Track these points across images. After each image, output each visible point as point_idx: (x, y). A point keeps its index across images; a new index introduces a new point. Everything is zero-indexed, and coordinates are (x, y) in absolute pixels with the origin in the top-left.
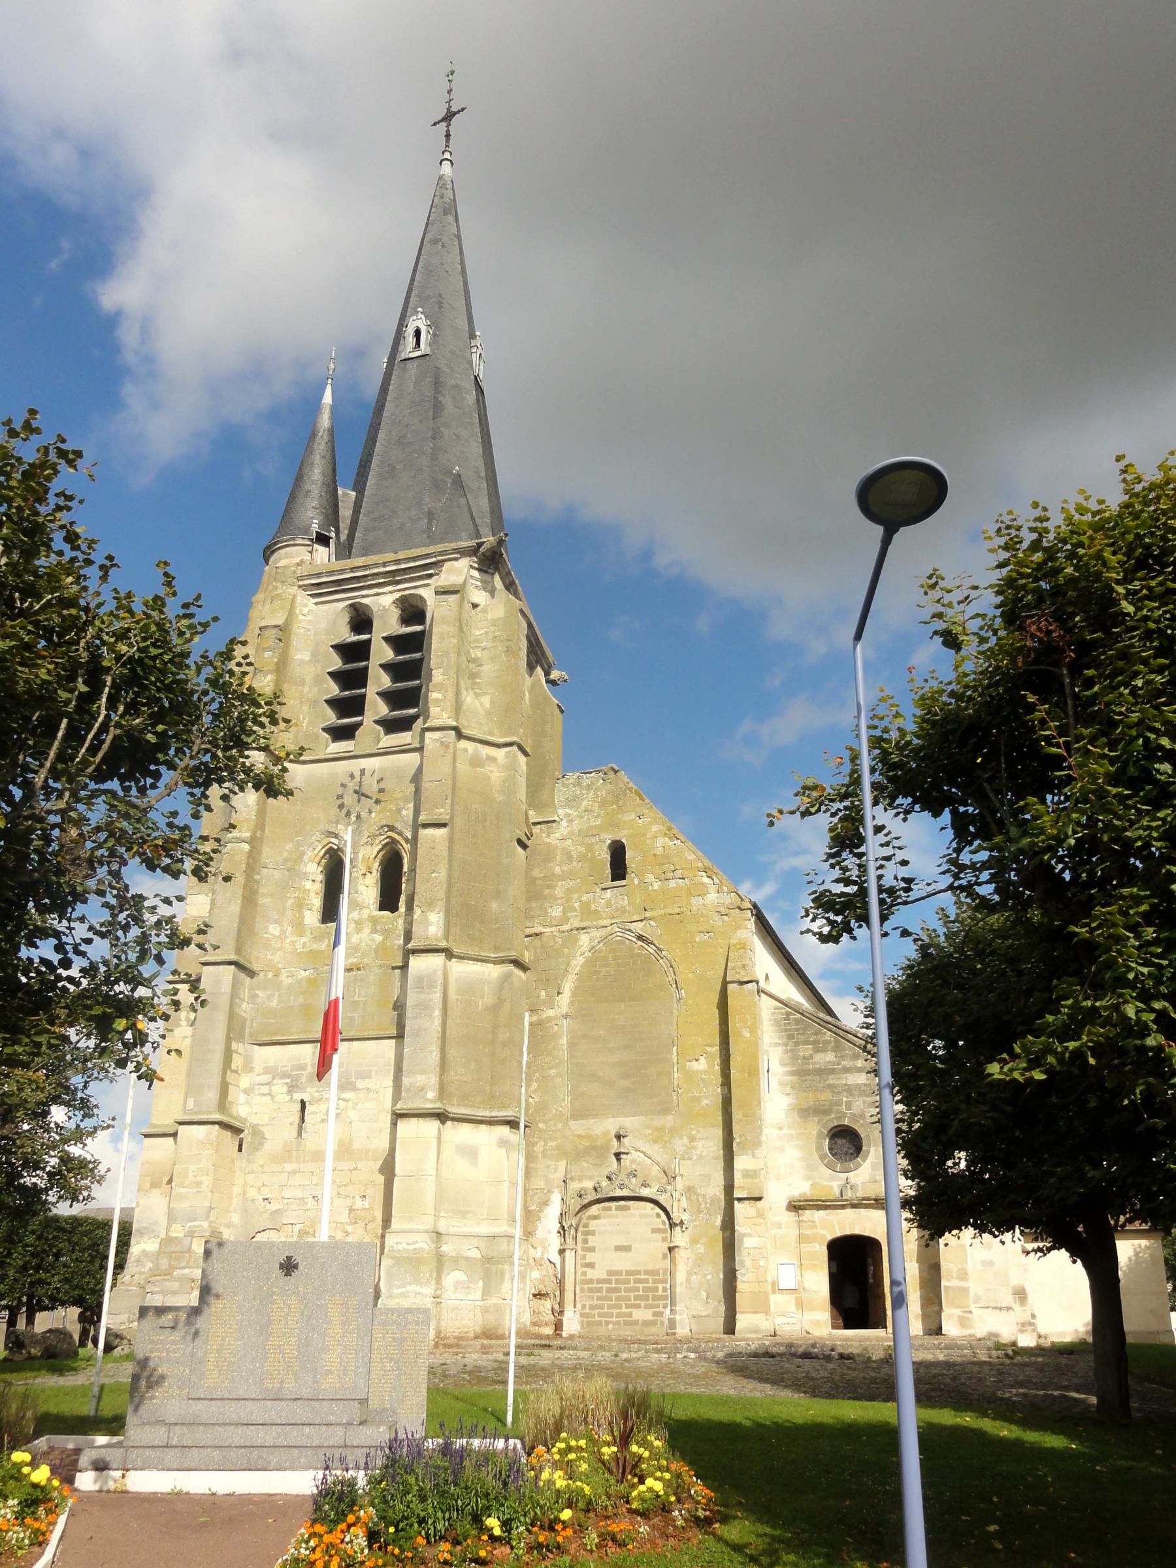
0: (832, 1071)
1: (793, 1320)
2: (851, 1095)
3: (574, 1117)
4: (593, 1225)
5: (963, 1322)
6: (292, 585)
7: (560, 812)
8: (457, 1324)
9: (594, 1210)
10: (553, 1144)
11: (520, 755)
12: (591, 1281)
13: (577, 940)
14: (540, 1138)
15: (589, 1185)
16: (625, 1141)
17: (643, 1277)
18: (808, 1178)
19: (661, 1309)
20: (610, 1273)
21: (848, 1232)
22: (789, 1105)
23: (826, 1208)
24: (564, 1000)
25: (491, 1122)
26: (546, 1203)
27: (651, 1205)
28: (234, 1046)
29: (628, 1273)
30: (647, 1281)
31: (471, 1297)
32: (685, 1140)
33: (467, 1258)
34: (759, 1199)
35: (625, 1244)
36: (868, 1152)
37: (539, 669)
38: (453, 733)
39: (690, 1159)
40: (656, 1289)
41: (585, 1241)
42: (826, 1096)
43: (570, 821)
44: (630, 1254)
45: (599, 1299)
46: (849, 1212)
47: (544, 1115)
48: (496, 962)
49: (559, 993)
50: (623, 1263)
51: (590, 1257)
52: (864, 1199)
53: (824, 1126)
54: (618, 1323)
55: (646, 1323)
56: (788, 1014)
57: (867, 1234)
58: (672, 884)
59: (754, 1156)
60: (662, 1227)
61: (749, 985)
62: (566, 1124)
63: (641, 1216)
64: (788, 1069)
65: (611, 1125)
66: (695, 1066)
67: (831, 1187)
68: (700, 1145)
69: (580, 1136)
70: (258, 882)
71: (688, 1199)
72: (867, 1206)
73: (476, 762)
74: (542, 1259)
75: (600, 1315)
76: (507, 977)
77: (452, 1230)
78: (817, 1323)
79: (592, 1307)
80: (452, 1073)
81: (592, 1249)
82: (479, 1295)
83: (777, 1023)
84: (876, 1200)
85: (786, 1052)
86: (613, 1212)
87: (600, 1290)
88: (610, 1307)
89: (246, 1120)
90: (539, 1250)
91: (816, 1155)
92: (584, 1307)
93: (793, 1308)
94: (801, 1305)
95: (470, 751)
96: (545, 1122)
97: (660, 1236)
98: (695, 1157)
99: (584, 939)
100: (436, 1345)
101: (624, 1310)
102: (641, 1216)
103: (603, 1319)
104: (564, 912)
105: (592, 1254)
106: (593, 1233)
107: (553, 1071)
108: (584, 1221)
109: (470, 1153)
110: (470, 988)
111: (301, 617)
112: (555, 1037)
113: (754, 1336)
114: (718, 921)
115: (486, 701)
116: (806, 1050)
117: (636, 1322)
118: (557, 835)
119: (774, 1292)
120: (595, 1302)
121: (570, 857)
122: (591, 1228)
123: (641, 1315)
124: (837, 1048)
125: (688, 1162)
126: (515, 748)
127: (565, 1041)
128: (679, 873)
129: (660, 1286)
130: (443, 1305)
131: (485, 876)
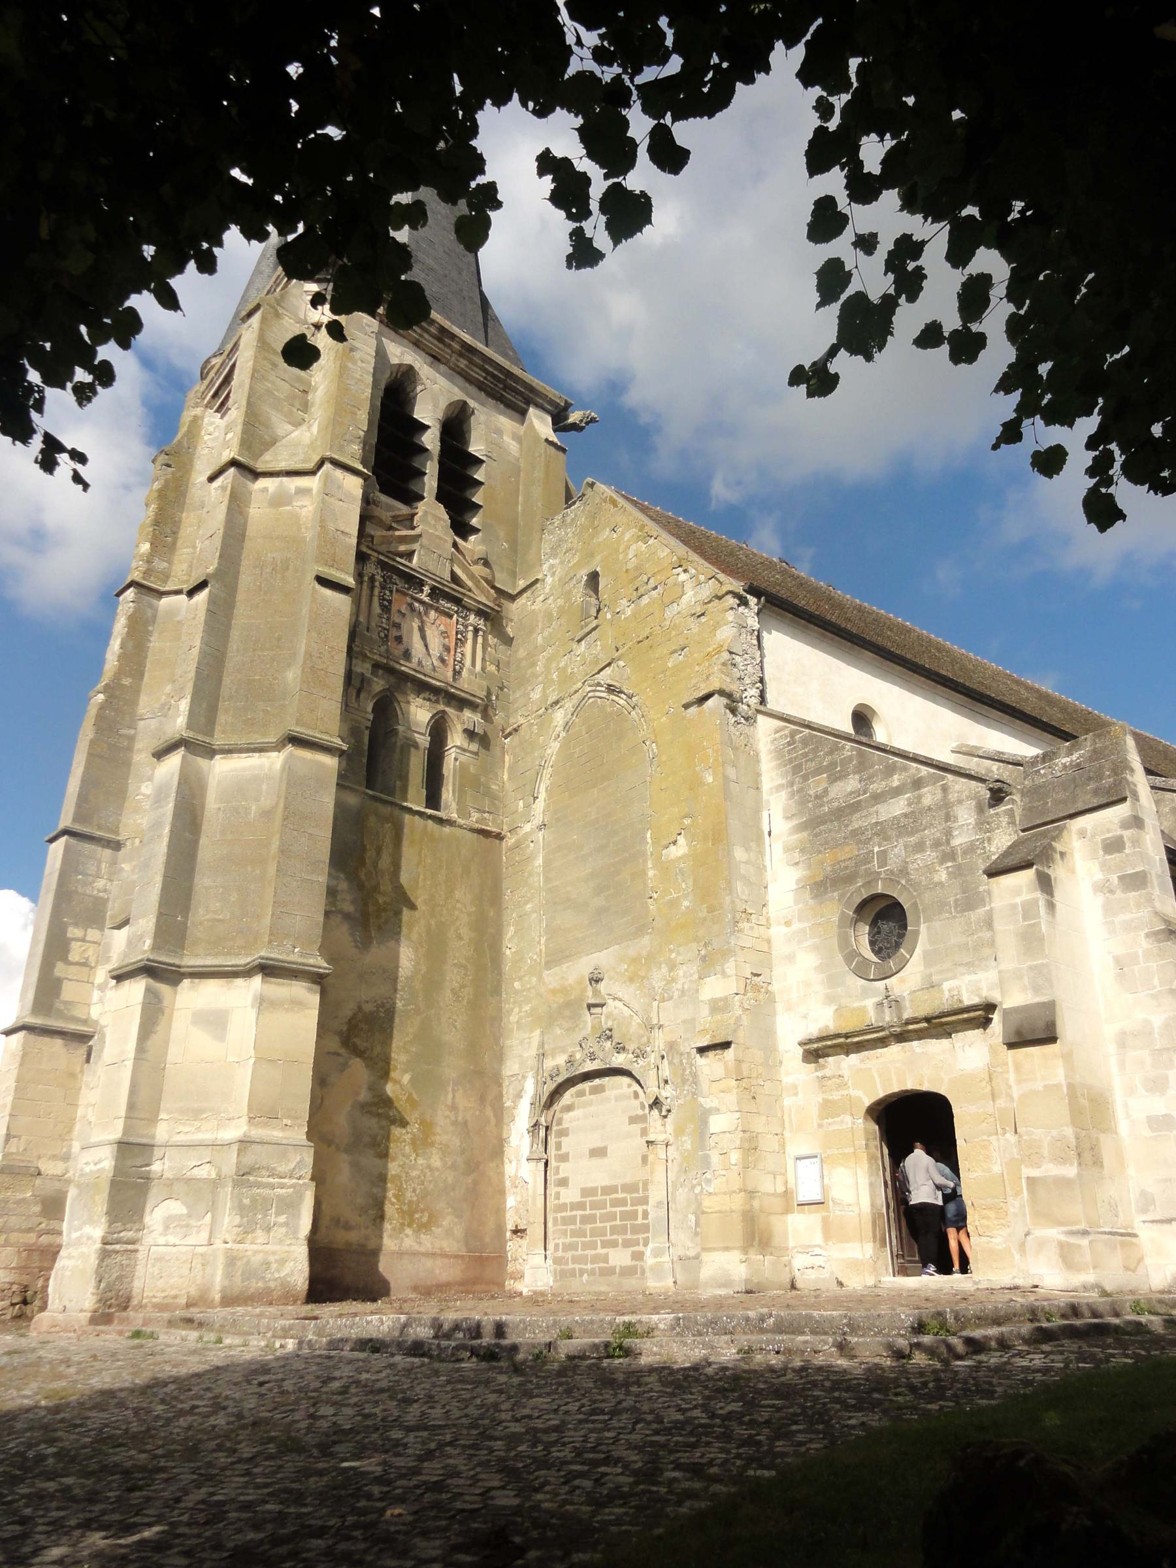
0: (855, 807)
1: (818, 1261)
2: (887, 838)
3: (549, 965)
4: (567, 1117)
5: (1067, 1257)
6: (197, 405)
7: (545, 567)
8: (160, 1283)
9: (568, 1097)
10: (527, 1008)
11: (339, 473)
12: (561, 1208)
13: (551, 720)
14: (515, 1002)
15: (561, 1060)
16: (602, 986)
17: (620, 1195)
18: (830, 999)
19: (641, 1248)
20: (586, 1192)
21: (895, 1088)
22: (798, 881)
23: (859, 1047)
24: (539, 806)
25: (246, 973)
26: (519, 1096)
27: (626, 1080)
28: (73, 932)
29: (607, 1190)
30: (623, 1202)
31: (191, 1240)
32: (664, 969)
33: (189, 1180)
34: (726, 1045)
36: (916, 933)
37: (532, 411)
38: (232, 470)
39: (670, 998)
40: (633, 1215)
41: (559, 1146)
42: (850, 851)
43: (553, 574)
44: (606, 1161)
45: (574, 1234)
46: (895, 1049)
48: (278, 747)
49: (535, 798)
50: (597, 1175)
51: (565, 1169)
52: (909, 1022)
53: (847, 904)
54: (592, 1273)
55: (628, 1272)
56: (793, 734)
57: (926, 1087)
58: (645, 600)
59: (724, 974)
60: (640, 1112)
61: (710, 702)
62: (540, 978)
63: (617, 1099)
64: (795, 822)
65: (583, 966)
66: (675, 852)
67: (863, 1009)
68: (681, 973)
69: (554, 992)
70: (132, 739)
71: (670, 1063)
72: (920, 1035)
73: (279, 500)
75: (575, 1260)
76: (288, 767)
77: (177, 1139)
78: (855, 1265)
79: (568, 1247)
80: (201, 911)
81: (564, 1158)
82: (204, 1236)
83: (778, 753)
84: (928, 1020)
85: (792, 794)
86: (588, 1097)
87: (572, 1221)
88: (586, 1246)
89: (97, 1022)
90: (514, 1163)
91: (839, 958)
92: (557, 1246)
93: (818, 1238)
94: (829, 1230)
95: (271, 490)
96: (520, 979)
97: (637, 1128)
98: (676, 993)
99: (559, 717)
100: (101, 1318)
101: (600, 1251)
102: (617, 1099)
103: (577, 1266)
104: (544, 689)
106: (564, 1133)
107: (529, 906)
108: (558, 1115)
109: (216, 1022)
110: (239, 789)
111: (206, 438)
112: (530, 859)
113: (722, 1292)
114: (694, 626)
115: (315, 429)
116: (818, 783)
117: (610, 1271)
118: (541, 598)
119: (787, 1210)
120: (569, 1240)
121: (549, 616)
122: (565, 1125)
123: (619, 1258)
124: (862, 765)
125: (669, 1004)
126: (327, 466)
127: (539, 861)
128: (652, 583)
129: (640, 1209)
130: (141, 1256)
131: (279, 639)
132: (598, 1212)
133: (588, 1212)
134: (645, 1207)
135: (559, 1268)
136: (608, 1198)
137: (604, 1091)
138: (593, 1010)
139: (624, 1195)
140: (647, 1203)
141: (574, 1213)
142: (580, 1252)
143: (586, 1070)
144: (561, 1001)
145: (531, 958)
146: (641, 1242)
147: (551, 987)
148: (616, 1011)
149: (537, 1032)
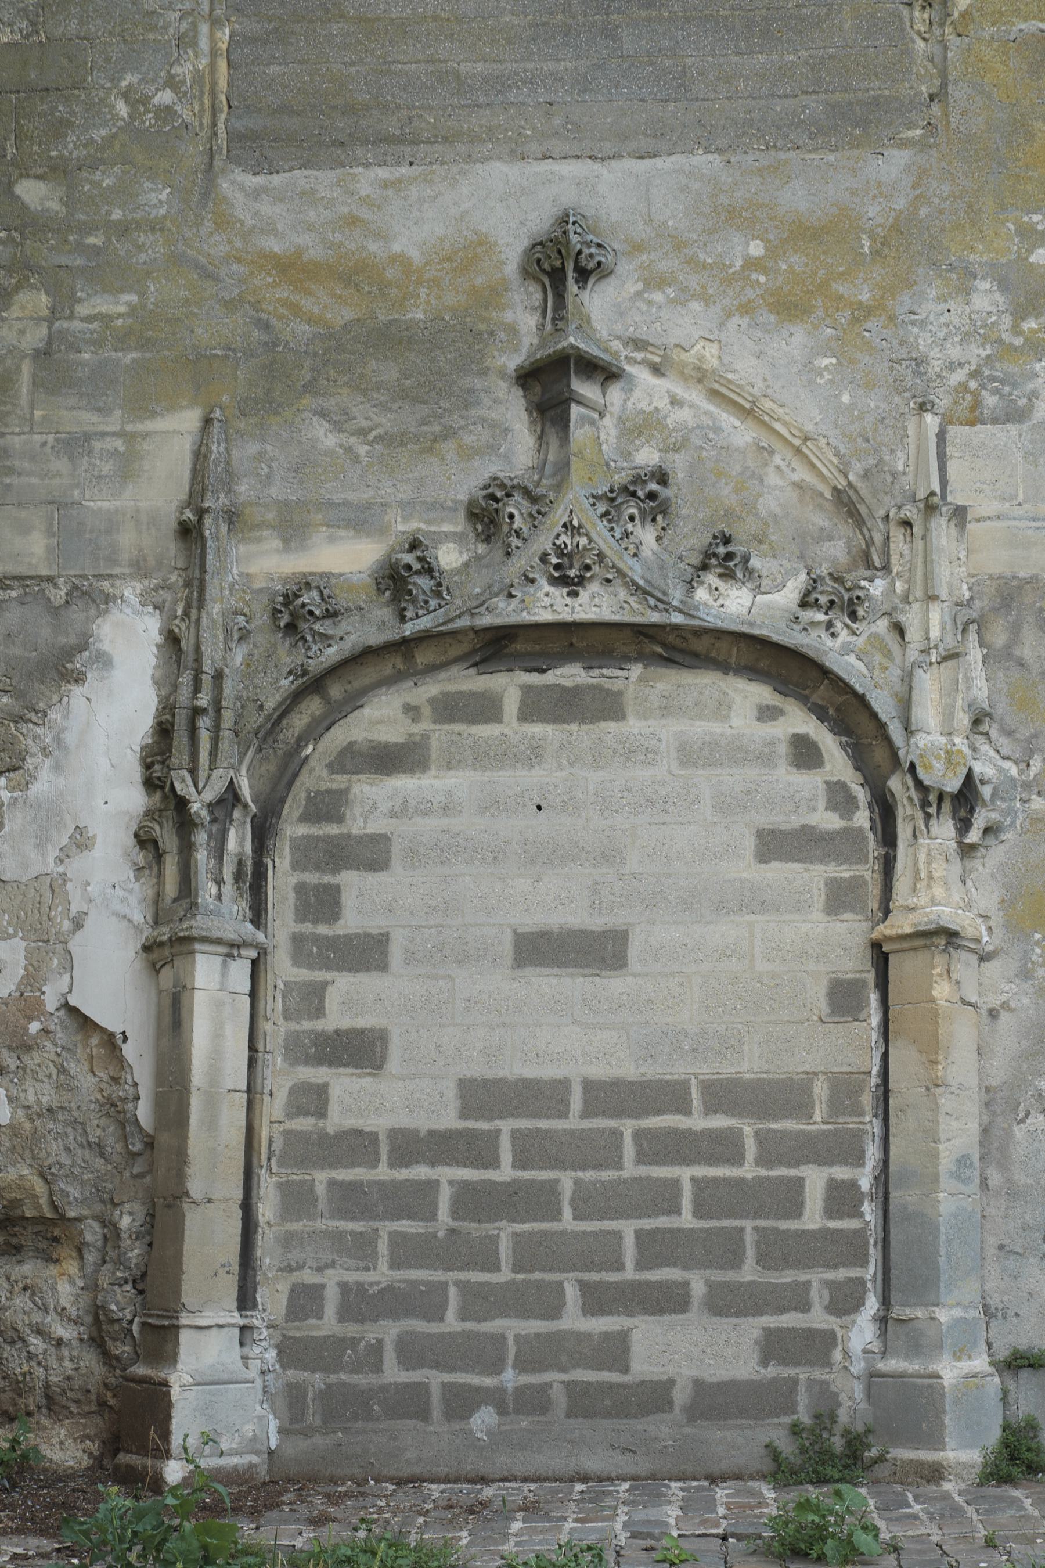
17: (698, 1122)
19: (818, 1318)
35: (597, 923)
44: (615, 985)
47: (59, 129)
60: (832, 821)
74: (32, 1008)
103: (435, 1379)
105: (367, 983)
122: (356, 825)
132: (566, 1181)
133: (505, 1172)
134: (841, 1173)
135: (317, 1380)
136: (628, 1127)
137: (619, 715)
138: (585, 389)
139: (720, 1122)
140: (859, 1160)
141: (421, 1172)
142: (452, 1322)
143: (546, 616)
144: (348, 314)
145: (137, 100)
146: (818, 1297)
147: (274, 245)
148: (682, 416)
149: (189, 420)
